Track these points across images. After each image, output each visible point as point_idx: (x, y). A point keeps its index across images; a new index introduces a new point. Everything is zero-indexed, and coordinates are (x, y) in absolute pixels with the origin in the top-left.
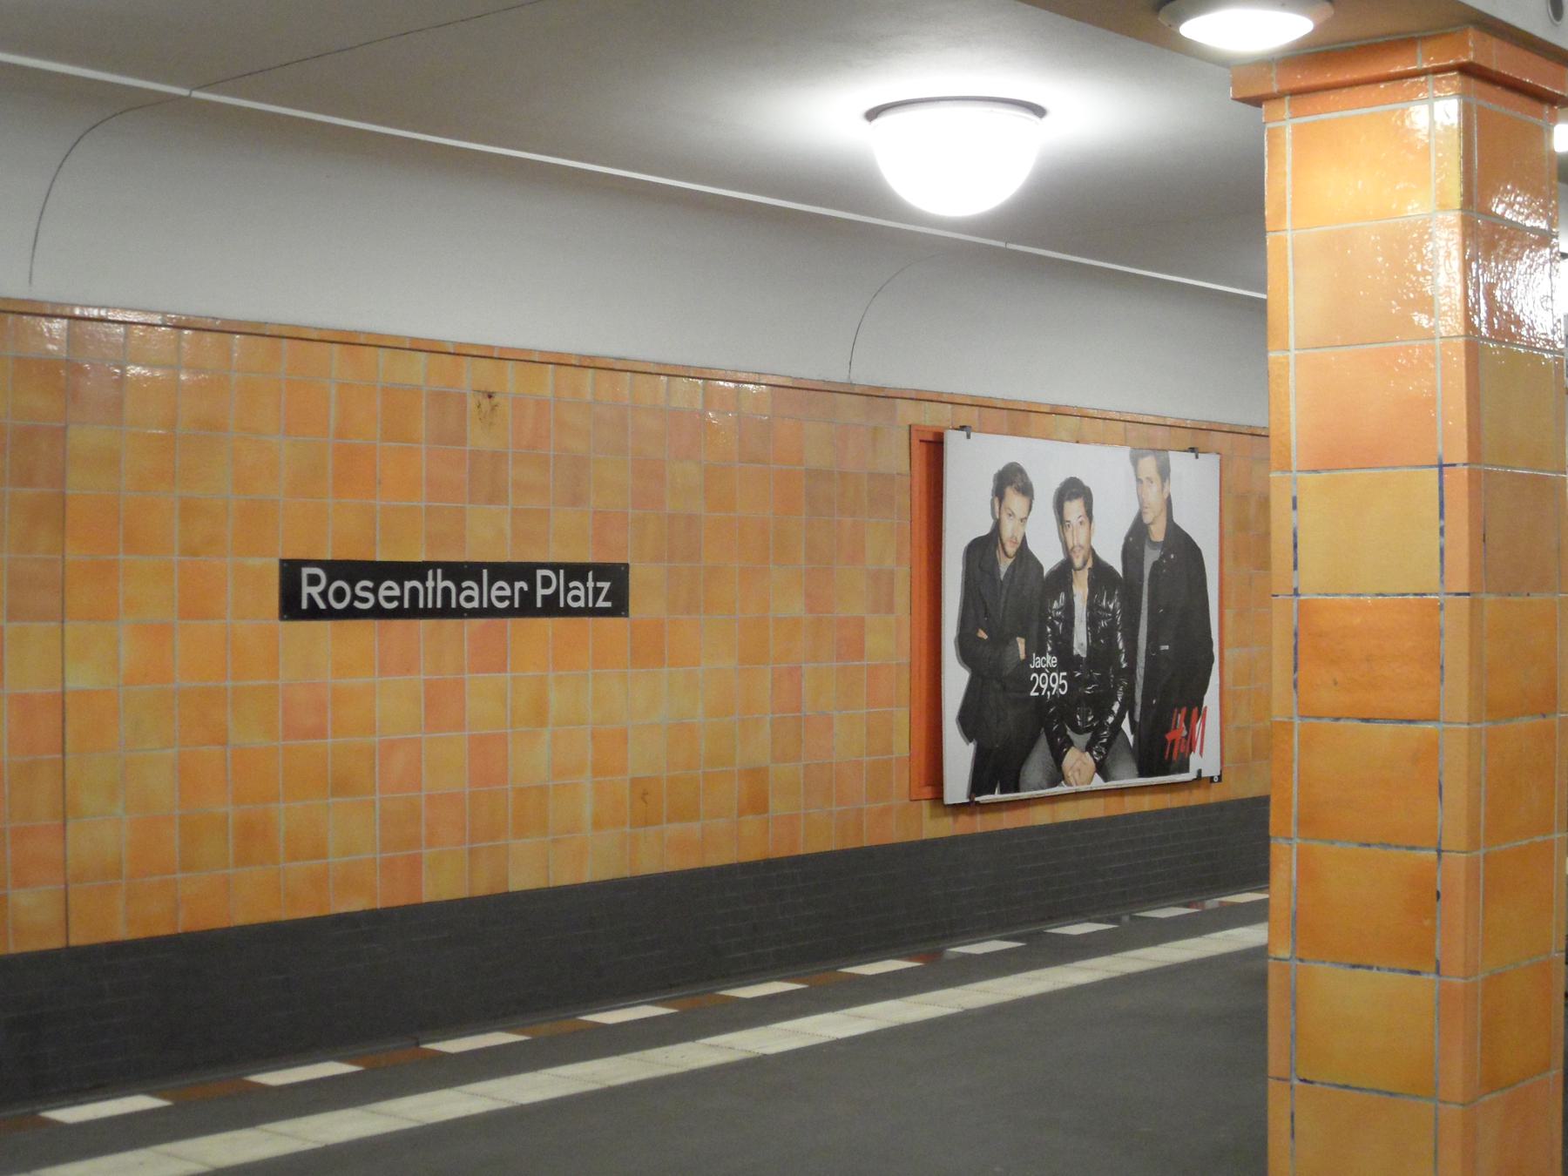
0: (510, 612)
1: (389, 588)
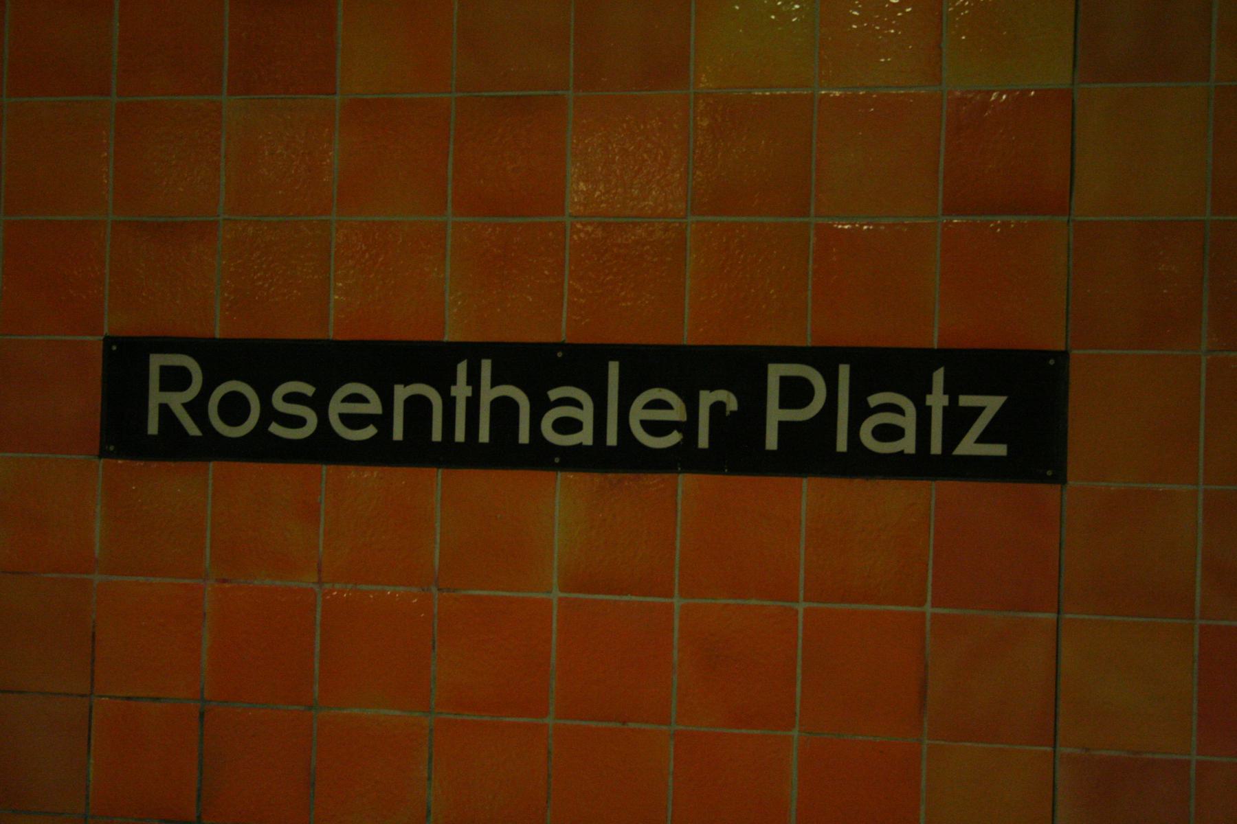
0: (685, 458)
1: (355, 399)
